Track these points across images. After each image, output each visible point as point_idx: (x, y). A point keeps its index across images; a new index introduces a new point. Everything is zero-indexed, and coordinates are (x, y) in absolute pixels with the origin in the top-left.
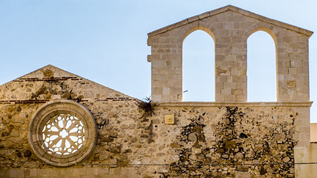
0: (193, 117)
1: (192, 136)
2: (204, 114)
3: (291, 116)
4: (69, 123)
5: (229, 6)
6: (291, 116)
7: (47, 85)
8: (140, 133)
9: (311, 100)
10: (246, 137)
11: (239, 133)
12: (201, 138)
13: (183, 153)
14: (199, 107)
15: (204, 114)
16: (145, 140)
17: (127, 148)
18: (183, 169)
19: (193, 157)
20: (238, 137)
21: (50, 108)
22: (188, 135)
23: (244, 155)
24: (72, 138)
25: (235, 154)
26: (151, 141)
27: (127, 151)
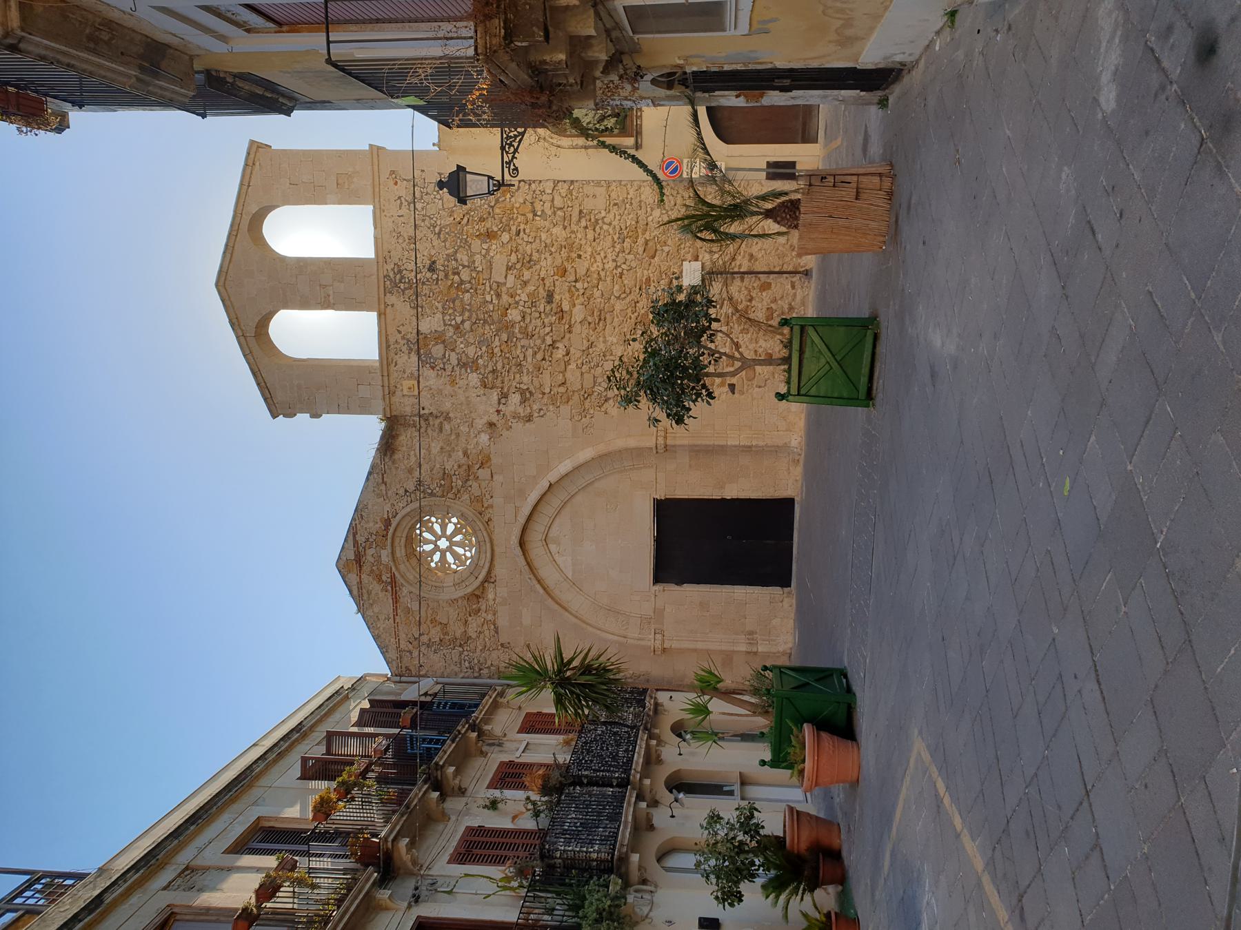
0: (405, 348)
1: (437, 350)
2: (399, 332)
3: (396, 183)
4: (426, 535)
5: (217, 285)
6: (396, 183)
7: (366, 568)
8: (435, 434)
9: (367, 148)
10: (434, 262)
11: (429, 275)
12: (439, 338)
13: (465, 365)
14: (387, 341)
15: (399, 332)
16: (447, 427)
17: (460, 454)
18: (490, 368)
19: (471, 351)
20: (435, 276)
21: (402, 567)
22: (436, 359)
23: (464, 267)
24: (449, 532)
25: (462, 282)
26: (448, 418)
27: (465, 454)
